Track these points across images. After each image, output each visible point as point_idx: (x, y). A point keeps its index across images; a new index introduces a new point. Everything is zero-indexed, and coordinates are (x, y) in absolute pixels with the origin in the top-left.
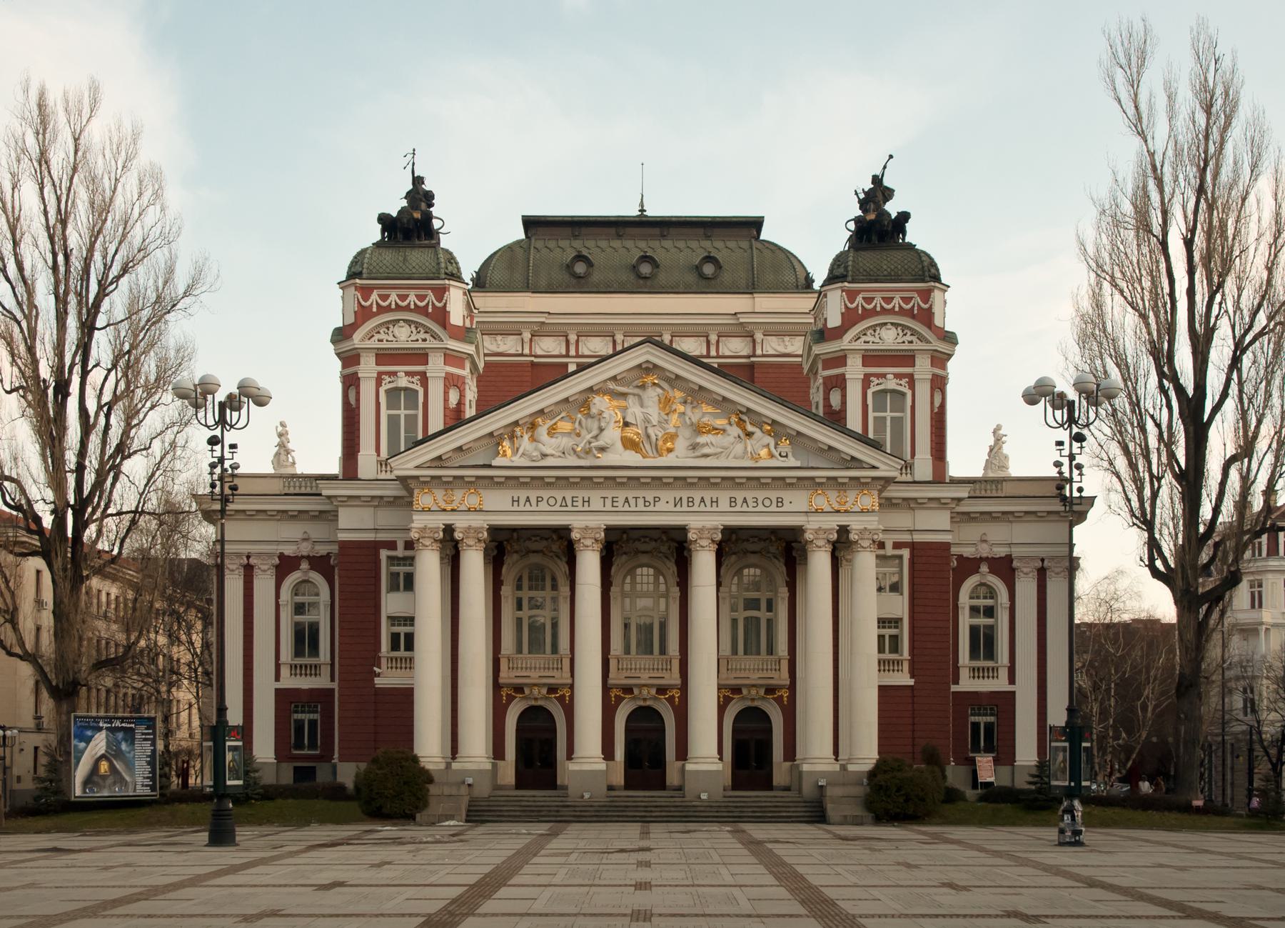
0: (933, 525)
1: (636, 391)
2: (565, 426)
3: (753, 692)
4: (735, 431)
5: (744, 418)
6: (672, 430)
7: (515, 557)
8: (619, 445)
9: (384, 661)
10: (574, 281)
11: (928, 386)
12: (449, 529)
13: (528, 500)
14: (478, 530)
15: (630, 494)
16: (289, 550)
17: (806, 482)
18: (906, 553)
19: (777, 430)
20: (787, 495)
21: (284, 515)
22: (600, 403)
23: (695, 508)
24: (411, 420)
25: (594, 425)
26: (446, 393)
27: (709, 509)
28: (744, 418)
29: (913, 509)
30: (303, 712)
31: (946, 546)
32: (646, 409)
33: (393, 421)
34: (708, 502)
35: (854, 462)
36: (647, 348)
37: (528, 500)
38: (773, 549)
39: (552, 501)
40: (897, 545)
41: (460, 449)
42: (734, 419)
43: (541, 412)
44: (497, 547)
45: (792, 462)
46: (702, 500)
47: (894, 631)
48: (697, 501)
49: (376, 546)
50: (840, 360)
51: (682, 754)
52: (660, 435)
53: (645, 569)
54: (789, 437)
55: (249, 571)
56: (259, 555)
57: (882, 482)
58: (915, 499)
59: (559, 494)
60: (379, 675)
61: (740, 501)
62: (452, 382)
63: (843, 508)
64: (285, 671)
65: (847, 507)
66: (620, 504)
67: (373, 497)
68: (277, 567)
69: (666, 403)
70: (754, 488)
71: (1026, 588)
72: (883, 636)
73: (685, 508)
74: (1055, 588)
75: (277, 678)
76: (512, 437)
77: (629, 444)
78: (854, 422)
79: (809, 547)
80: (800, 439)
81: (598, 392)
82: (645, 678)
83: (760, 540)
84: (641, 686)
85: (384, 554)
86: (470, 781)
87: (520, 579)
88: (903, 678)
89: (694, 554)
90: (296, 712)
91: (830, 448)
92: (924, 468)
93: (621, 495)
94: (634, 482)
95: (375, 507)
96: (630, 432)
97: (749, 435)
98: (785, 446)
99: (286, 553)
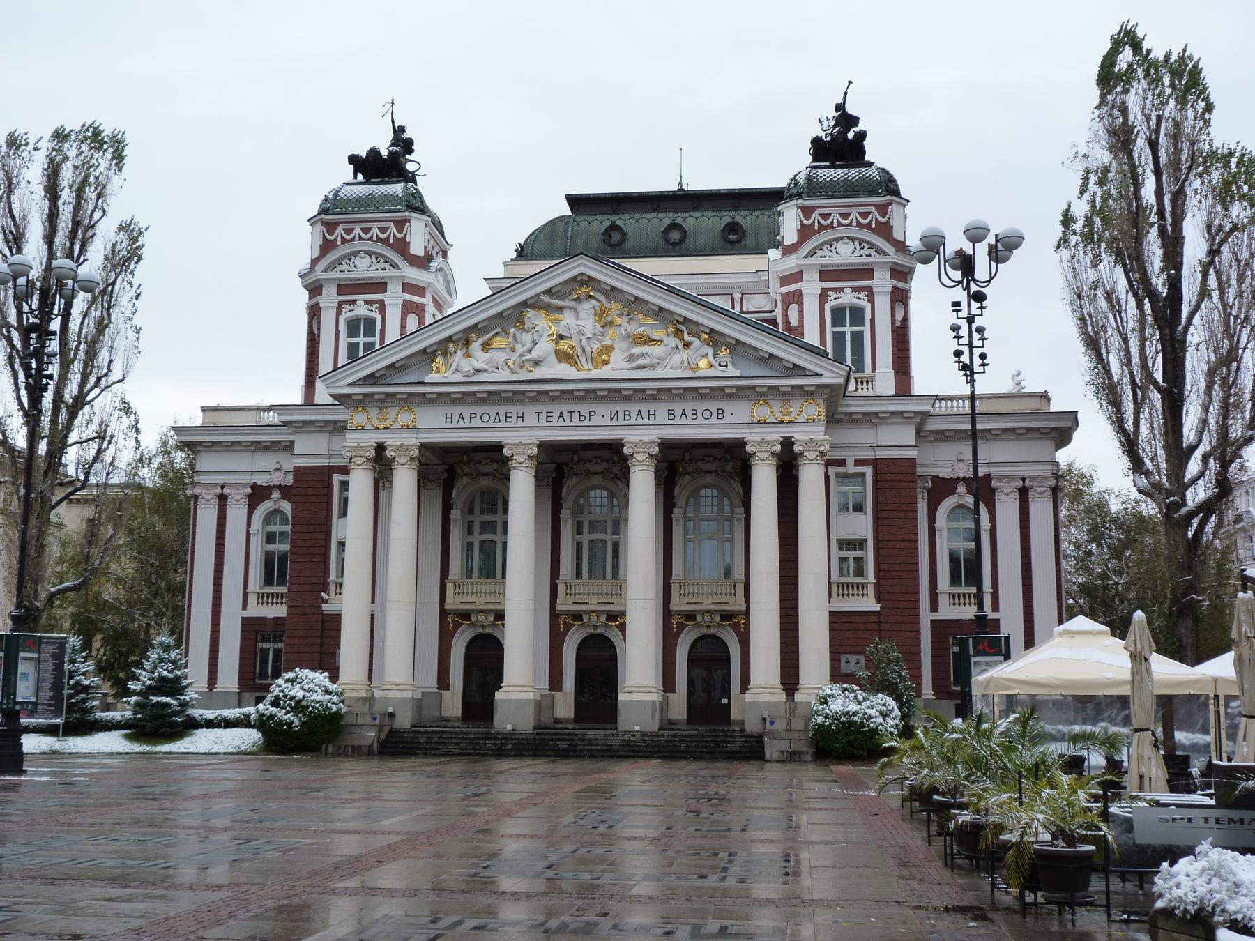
0: (897, 442)
1: (572, 304)
2: (501, 341)
3: (708, 618)
4: (673, 341)
5: (682, 327)
6: (608, 342)
7: (465, 480)
8: (553, 357)
9: (332, 588)
10: (608, 249)
11: (888, 299)
12: (380, 448)
13: (461, 416)
14: (407, 448)
15: (565, 408)
16: (262, 481)
17: (748, 393)
18: (869, 470)
19: (715, 340)
20: (728, 407)
21: (257, 447)
22: (536, 318)
23: (632, 422)
24: (369, 346)
25: (527, 338)
26: (404, 320)
27: (646, 422)
28: (682, 327)
29: (875, 425)
30: (269, 641)
31: (911, 463)
32: (580, 321)
33: (353, 348)
34: (645, 415)
35: (797, 370)
36: (582, 260)
37: (461, 416)
38: (729, 468)
39: (485, 418)
40: (859, 462)
41: (393, 365)
42: (671, 329)
43: (474, 328)
44: (447, 471)
45: (731, 371)
46: (640, 413)
47: (858, 553)
48: (634, 415)
49: (329, 471)
50: (798, 276)
52: (595, 347)
53: (598, 491)
54: (729, 346)
55: (223, 499)
56: (232, 485)
57: (828, 391)
58: (877, 414)
59: (492, 411)
60: (326, 601)
61: (678, 413)
62: (408, 308)
63: (786, 418)
64: (252, 600)
65: (791, 417)
66: (555, 419)
67: (327, 422)
68: (250, 497)
69: (601, 314)
70: (694, 400)
71: (1007, 509)
72: (846, 559)
73: (621, 422)
74: (1040, 509)
75: (244, 607)
76: (446, 354)
77: (563, 357)
78: (811, 336)
79: (753, 461)
80: (740, 348)
81: (532, 307)
82: (593, 604)
83: (715, 459)
84: (590, 612)
85: (337, 479)
86: (390, 710)
87: (472, 503)
88: (868, 603)
89: (631, 470)
90: (262, 641)
91: (771, 356)
92: (885, 382)
93: (556, 409)
94: (565, 396)
95: (330, 432)
96: (564, 346)
97: (687, 345)
98: (724, 355)
99: (259, 483)
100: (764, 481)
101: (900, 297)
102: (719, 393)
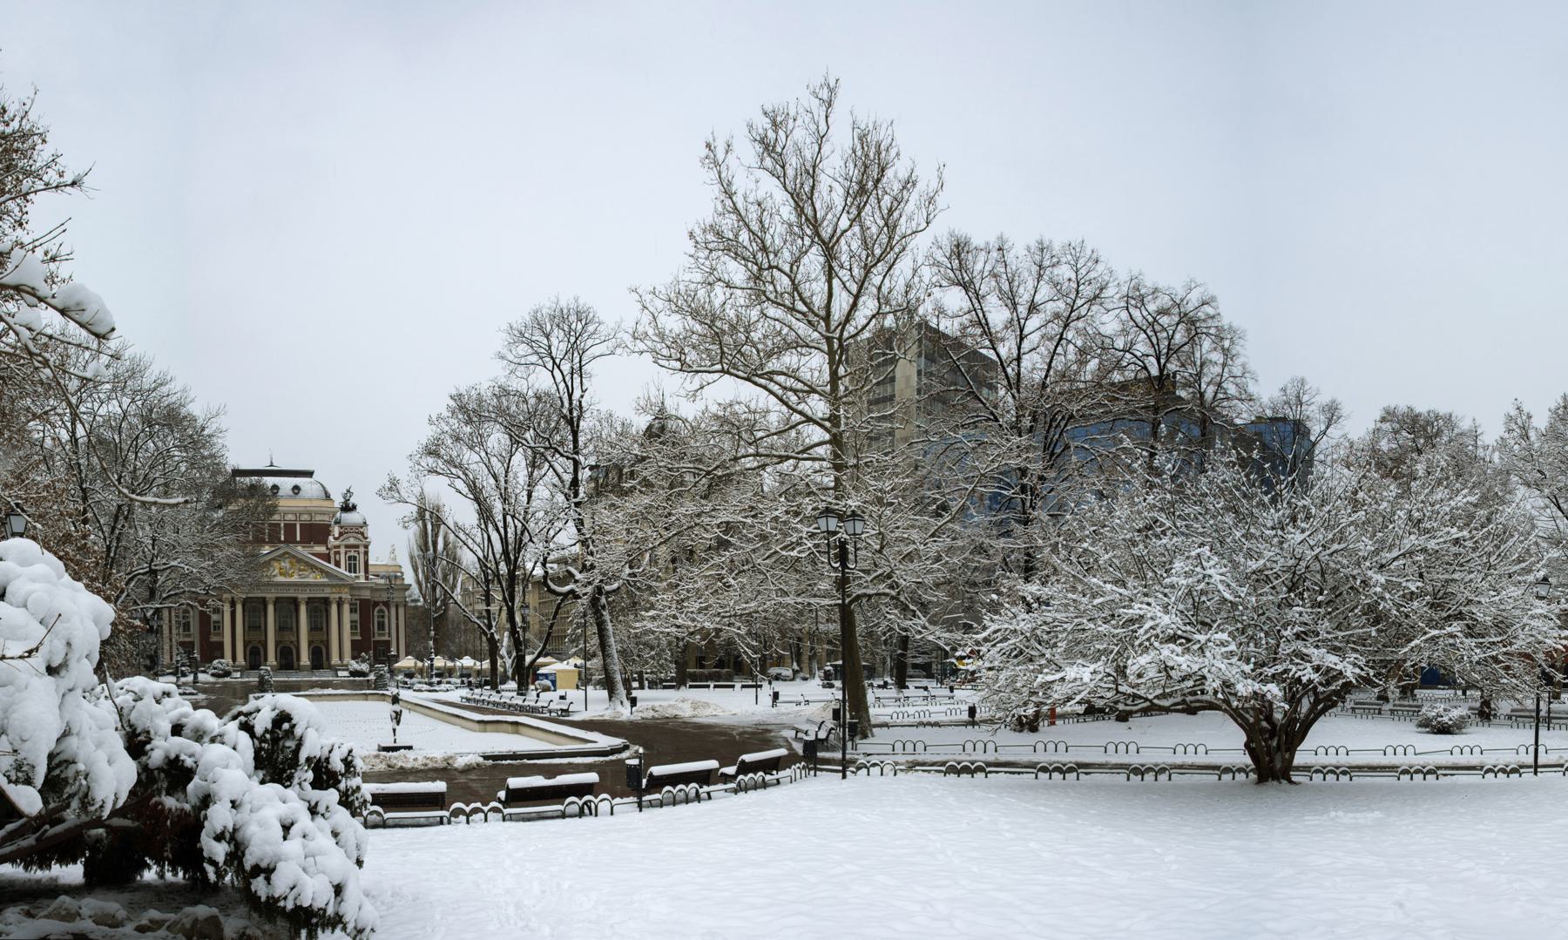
0: (366, 595)
32: (286, 564)
51: (298, 659)
71: (393, 610)
74: (401, 611)
100: (334, 608)
101: (366, 553)
102: (324, 585)
